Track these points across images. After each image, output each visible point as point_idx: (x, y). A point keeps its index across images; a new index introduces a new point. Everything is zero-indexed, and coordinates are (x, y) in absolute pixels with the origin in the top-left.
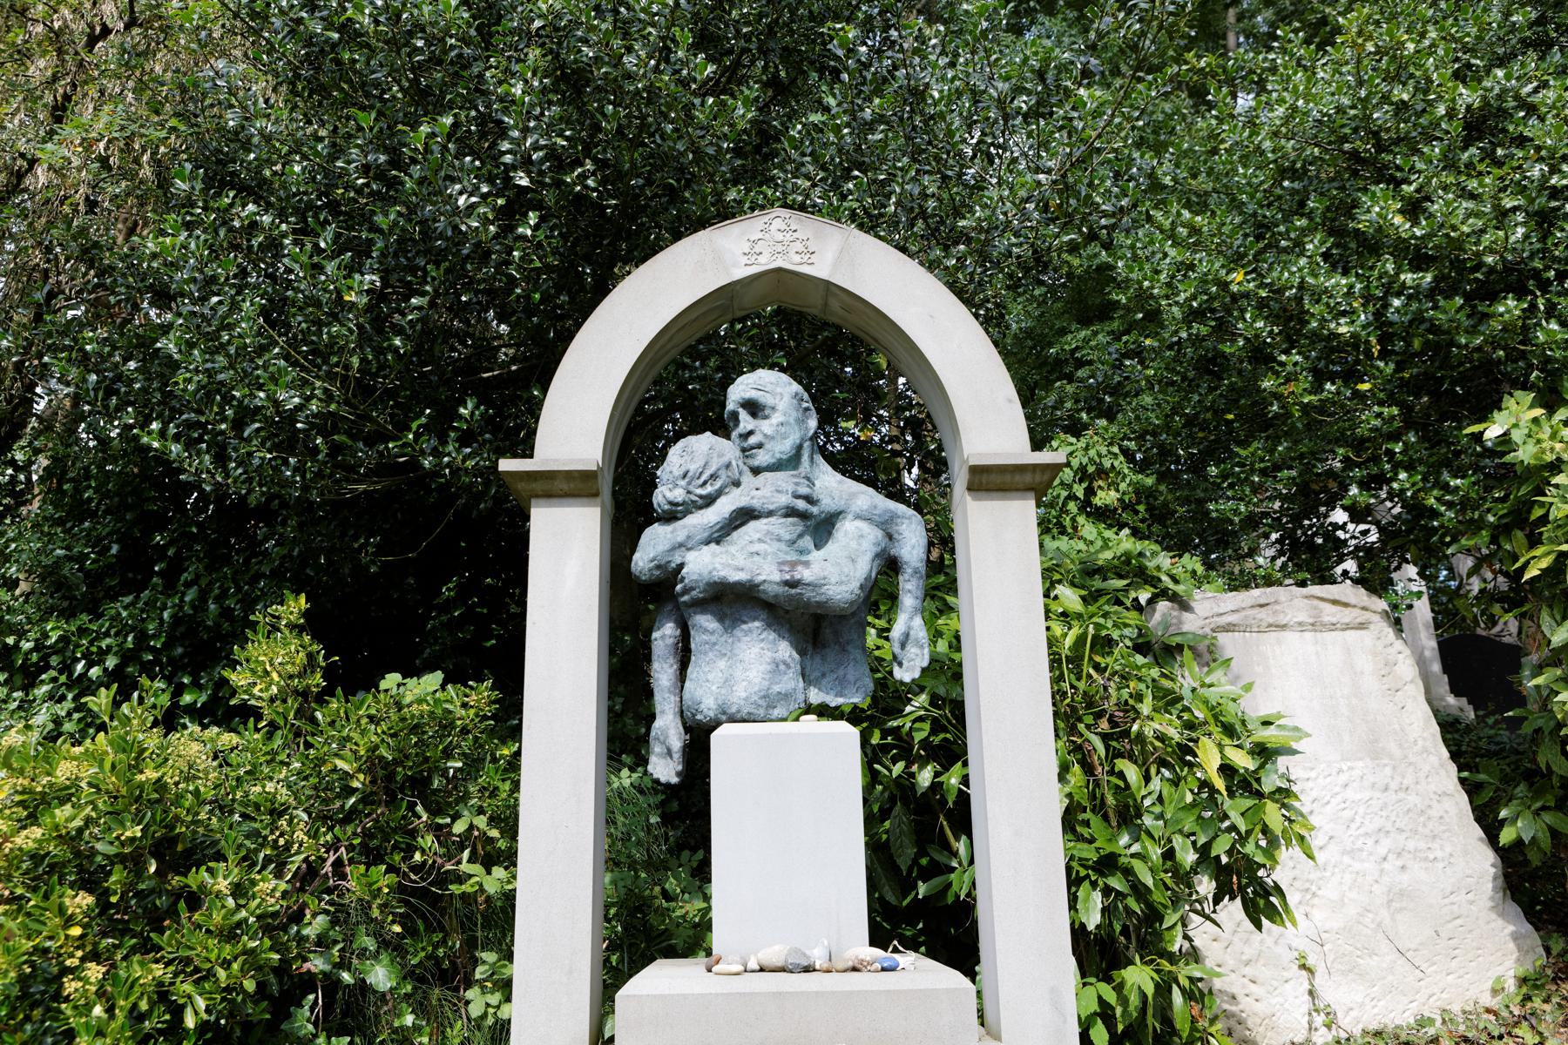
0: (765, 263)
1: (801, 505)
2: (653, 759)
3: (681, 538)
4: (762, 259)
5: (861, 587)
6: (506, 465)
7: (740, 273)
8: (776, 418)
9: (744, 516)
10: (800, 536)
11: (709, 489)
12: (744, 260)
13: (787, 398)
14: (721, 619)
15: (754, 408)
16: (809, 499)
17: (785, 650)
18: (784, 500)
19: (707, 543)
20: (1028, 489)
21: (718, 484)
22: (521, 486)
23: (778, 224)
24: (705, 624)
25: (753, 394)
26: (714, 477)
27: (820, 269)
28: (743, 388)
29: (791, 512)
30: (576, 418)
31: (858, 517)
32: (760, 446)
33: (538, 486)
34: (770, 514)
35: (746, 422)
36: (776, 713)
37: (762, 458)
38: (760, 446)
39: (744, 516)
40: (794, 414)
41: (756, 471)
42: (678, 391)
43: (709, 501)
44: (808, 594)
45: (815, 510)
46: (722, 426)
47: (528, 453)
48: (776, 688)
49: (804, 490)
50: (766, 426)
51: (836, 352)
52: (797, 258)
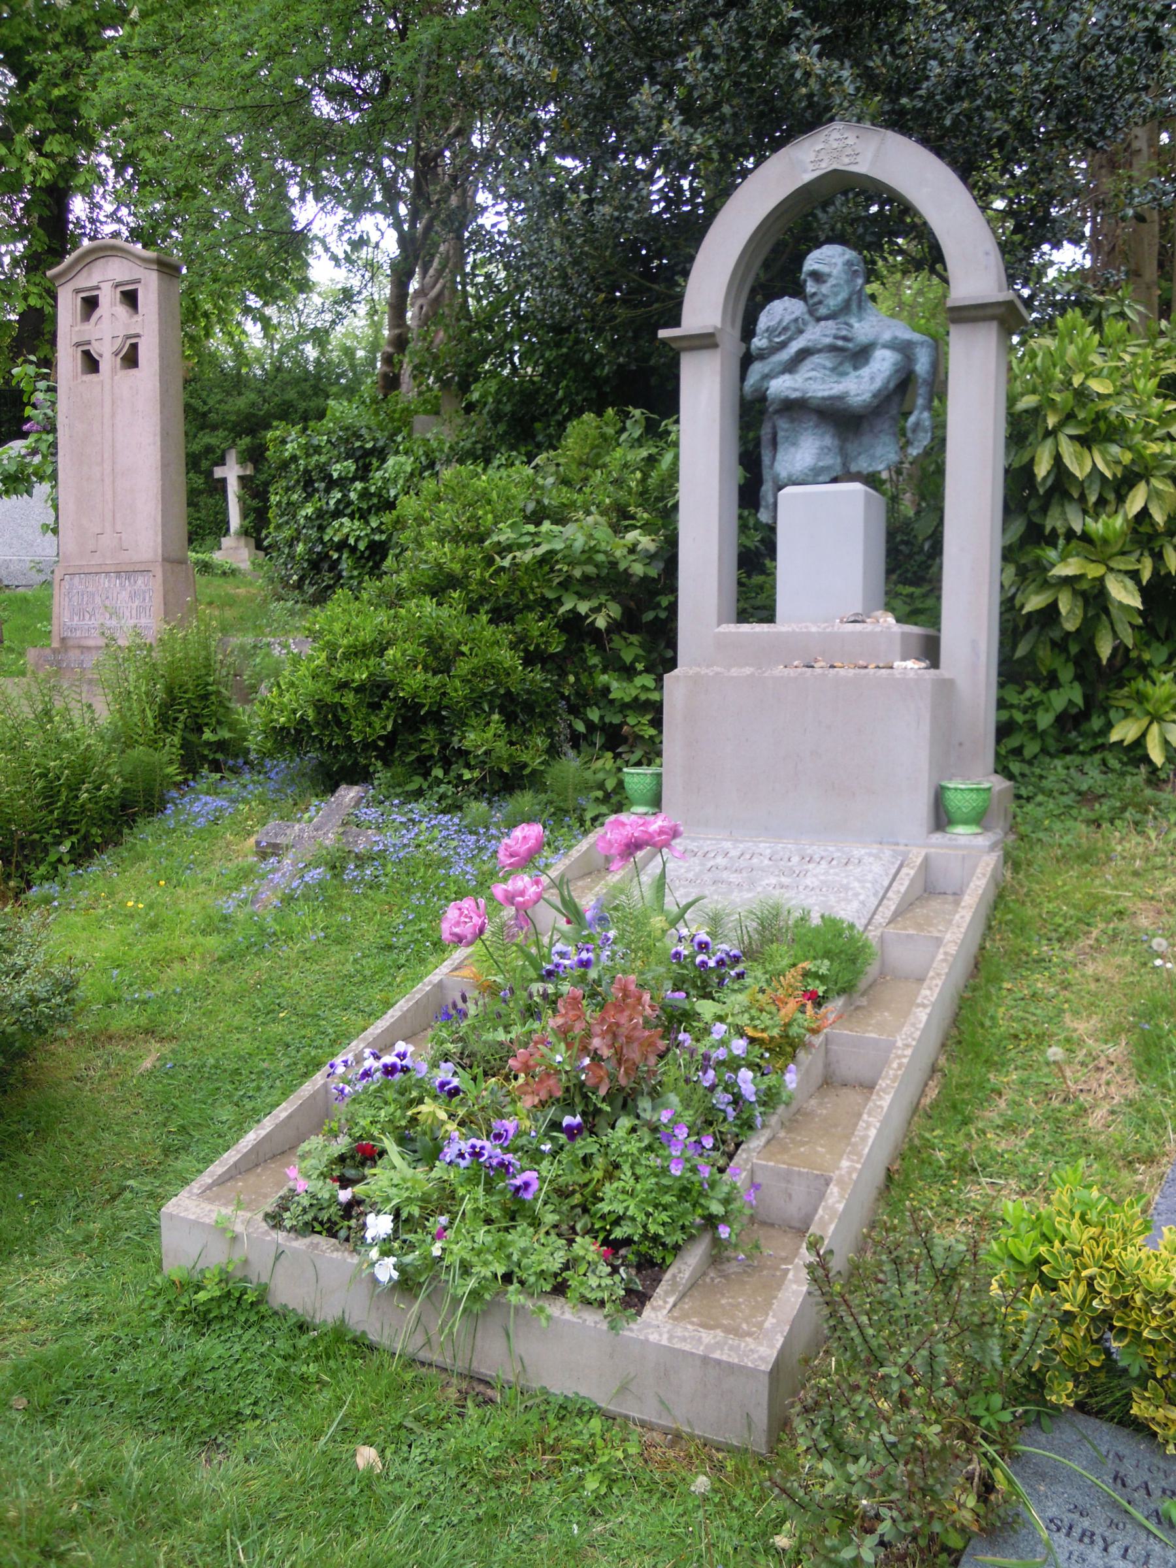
0: (825, 167)
1: (840, 343)
2: (762, 510)
3: (766, 370)
4: (823, 165)
5: (874, 396)
6: (663, 333)
7: (808, 177)
8: (832, 281)
9: (804, 354)
10: (841, 364)
11: (783, 338)
12: (811, 167)
13: (840, 267)
14: (792, 421)
15: (817, 276)
16: (845, 338)
17: (828, 441)
18: (828, 341)
19: (783, 372)
20: (992, 318)
21: (789, 334)
22: (674, 345)
23: (836, 135)
24: (783, 424)
25: (816, 267)
26: (786, 329)
27: (862, 167)
28: (814, 261)
29: (833, 348)
30: (706, 298)
31: (885, 346)
32: (820, 302)
33: (684, 344)
34: (819, 351)
35: (811, 287)
36: (821, 479)
37: (823, 311)
38: (820, 302)
39: (804, 354)
40: (844, 276)
41: (819, 320)
42: (775, 268)
43: (783, 345)
44: (838, 403)
45: (850, 345)
46: (797, 292)
47: (677, 323)
48: (821, 464)
49: (844, 333)
50: (825, 289)
51: (882, 227)
52: (846, 160)
